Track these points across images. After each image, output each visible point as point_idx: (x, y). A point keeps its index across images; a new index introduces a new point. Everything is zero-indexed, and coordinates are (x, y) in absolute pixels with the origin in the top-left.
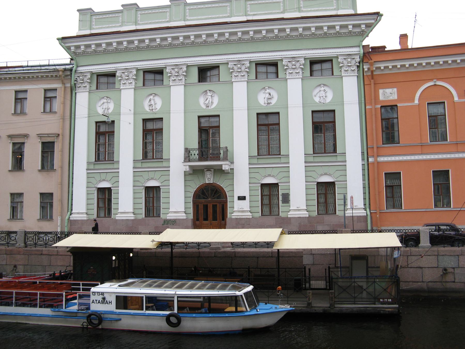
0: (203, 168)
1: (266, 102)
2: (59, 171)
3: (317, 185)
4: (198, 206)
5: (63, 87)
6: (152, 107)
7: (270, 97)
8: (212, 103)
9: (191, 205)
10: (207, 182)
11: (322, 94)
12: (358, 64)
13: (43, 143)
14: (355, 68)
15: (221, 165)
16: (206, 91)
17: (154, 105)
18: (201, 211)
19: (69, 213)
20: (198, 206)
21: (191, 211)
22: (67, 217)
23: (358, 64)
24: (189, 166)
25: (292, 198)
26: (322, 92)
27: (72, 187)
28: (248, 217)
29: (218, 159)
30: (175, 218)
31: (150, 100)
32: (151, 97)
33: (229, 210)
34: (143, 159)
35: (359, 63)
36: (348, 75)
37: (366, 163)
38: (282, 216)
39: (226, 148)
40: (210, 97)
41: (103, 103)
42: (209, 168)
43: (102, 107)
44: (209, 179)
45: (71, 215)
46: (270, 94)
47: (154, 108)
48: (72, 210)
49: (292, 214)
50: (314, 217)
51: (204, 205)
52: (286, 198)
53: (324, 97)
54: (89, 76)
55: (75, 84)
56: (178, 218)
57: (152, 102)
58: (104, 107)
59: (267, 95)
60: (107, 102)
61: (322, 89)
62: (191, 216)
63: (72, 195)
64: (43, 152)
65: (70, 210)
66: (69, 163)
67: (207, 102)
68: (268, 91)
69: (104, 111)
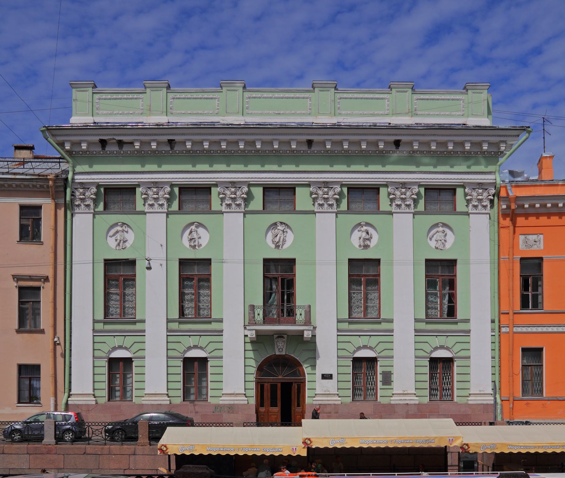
0: (272, 334)
1: (362, 244)
2: (49, 331)
3: (430, 361)
4: (262, 387)
5: (54, 203)
6: (195, 242)
7: (368, 237)
8: (284, 241)
9: (253, 385)
10: (277, 353)
11: (439, 236)
12: (492, 198)
13: (21, 289)
14: (487, 203)
15: (303, 331)
16: (275, 224)
17: (197, 239)
18: (267, 395)
19: (66, 394)
20: (262, 387)
21: (253, 393)
22: (64, 401)
23: (492, 198)
24: (255, 330)
25: (394, 377)
26: (441, 234)
27: (70, 356)
28: (336, 403)
29: (294, 323)
30: (232, 403)
31: (191, 232)
32: (193, 227)
33: (308, 393)
34: (180, 318)
35: (494, 196)
36: (477, 211)
37: (497, 333)
38: (382, 403)
39: (310, 306)
40: (281, 232)
41: (117, 232)
42: (280, 335)
43: (114, 238)
44: (281, 349)
45: (69, 397)
46: (368, 233)
47: (196, 243)
48: (70, 390)
49: (395, 400)
50: (425, 405)
51: (272, 385)
52: (387, 379)
53: (443, 241)
54: (94, 190)
55: (72, 201)
56: (236, 402)
57: (195, 235)
58: (119, 238)
59: (364, 234)
60: (123, 231)
61: (441, 229)
62: (253, 401)
63: (70, 367)
64: (21, 303)
65: (67, 390)
66: (65, 320)
67: (277, 239)
68: (365, 228)
69: (119, 244)
